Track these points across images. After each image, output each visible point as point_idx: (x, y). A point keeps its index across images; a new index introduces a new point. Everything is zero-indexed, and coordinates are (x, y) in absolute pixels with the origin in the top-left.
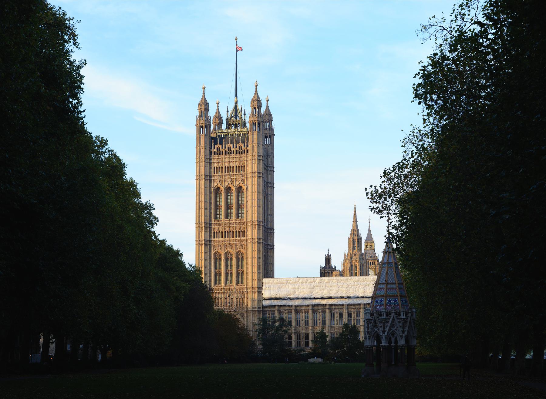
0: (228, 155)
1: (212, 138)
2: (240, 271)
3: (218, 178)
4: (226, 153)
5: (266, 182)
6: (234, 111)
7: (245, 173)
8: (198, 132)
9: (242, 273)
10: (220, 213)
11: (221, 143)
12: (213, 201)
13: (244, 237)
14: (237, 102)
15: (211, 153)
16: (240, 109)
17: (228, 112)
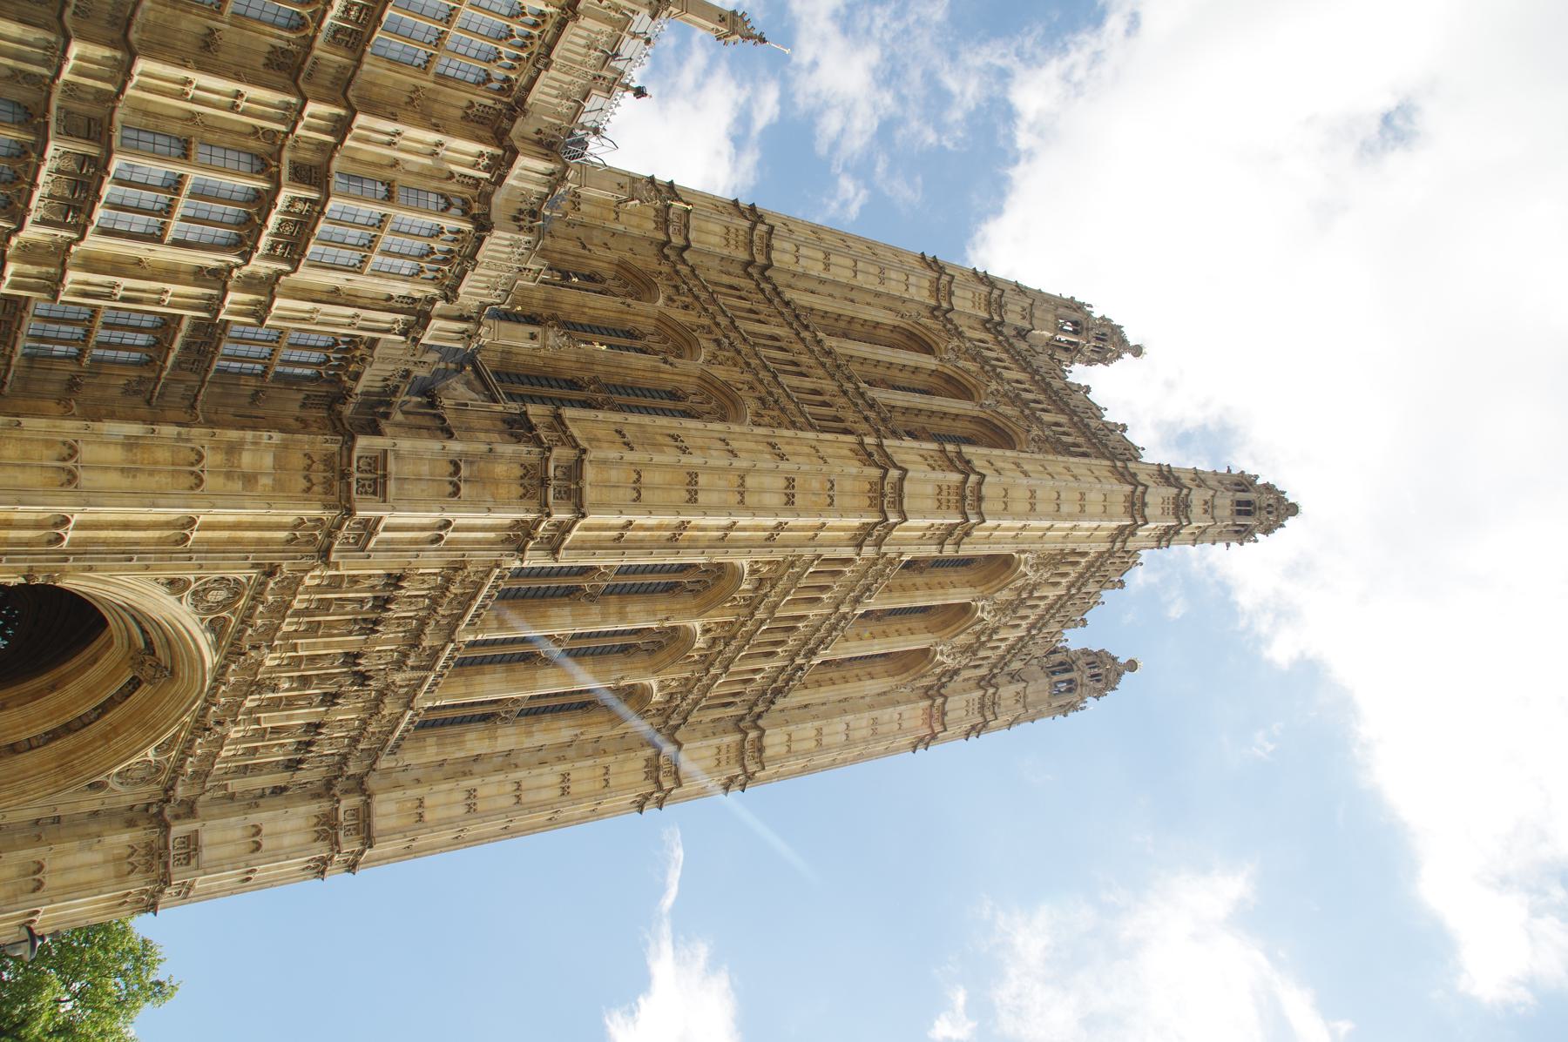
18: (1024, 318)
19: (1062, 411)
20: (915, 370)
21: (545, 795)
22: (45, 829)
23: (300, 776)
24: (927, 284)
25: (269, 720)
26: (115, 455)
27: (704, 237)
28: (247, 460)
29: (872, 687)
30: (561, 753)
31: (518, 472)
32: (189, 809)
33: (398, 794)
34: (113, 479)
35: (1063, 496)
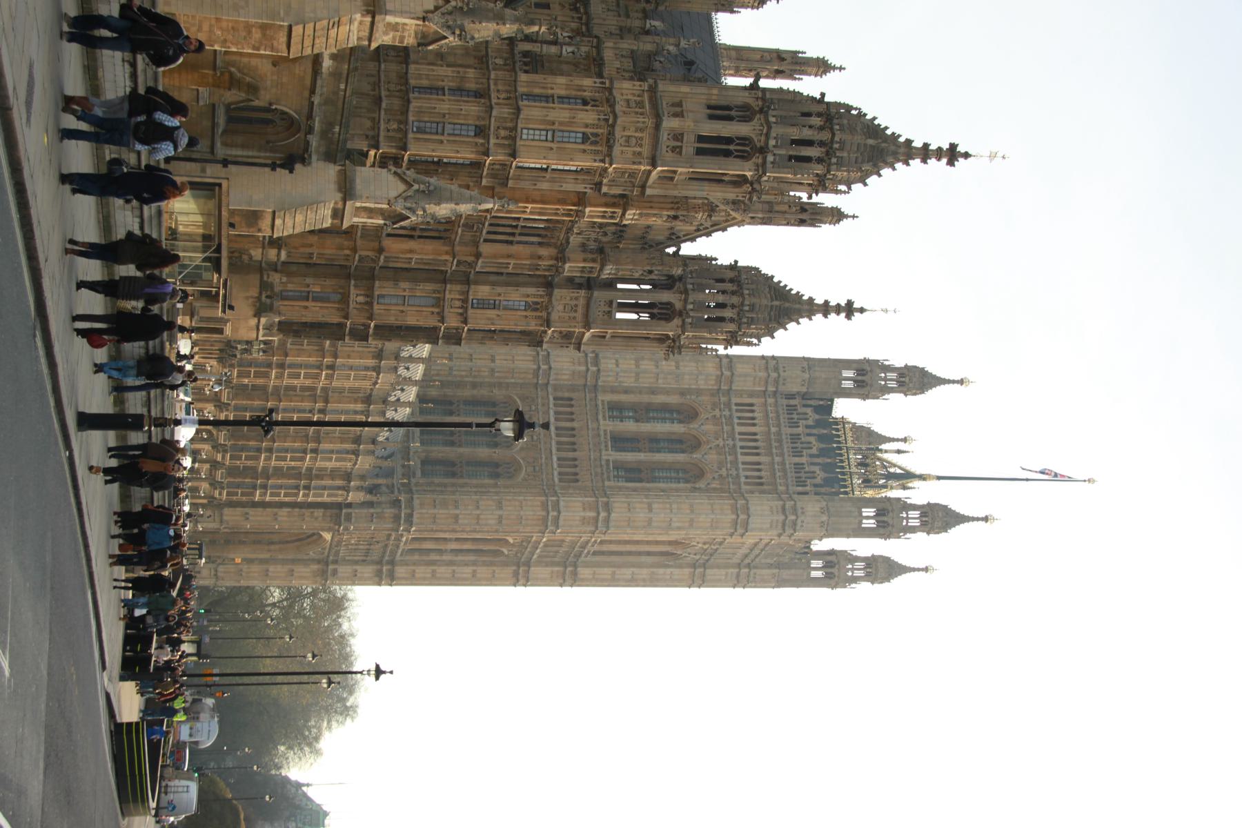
0: (789, 441)
1: (832, 401)
2: (461, 467)
3: (724, 413)
4: (795, 438)
5: (707, 561)
6: (899, 471)
7: (744, 487)
8: (847, 364)
9: (454, 475)
10: (626, 417)
11: (819, 424)
12: (660, 399)
13: (560, 480)
14: (924, 479)
15: (791, 396)
16: (910, 485)
17: (899, 452)
18: (803, 385)
19: (771, 454)
20: (674, 433)
21: (465, 576)
22: (294, 561)
23: (369, 558)
24: (714, 378)
25: (350, 547)
26: (285, 514)
27: (559, 377)
28: (316, 514)
29: (650, 559)
30: (474, 563)
31: (392, 515)
32: (335, 562)
33: (405, 567)
34: (285, 519)
35: (674, 519)
